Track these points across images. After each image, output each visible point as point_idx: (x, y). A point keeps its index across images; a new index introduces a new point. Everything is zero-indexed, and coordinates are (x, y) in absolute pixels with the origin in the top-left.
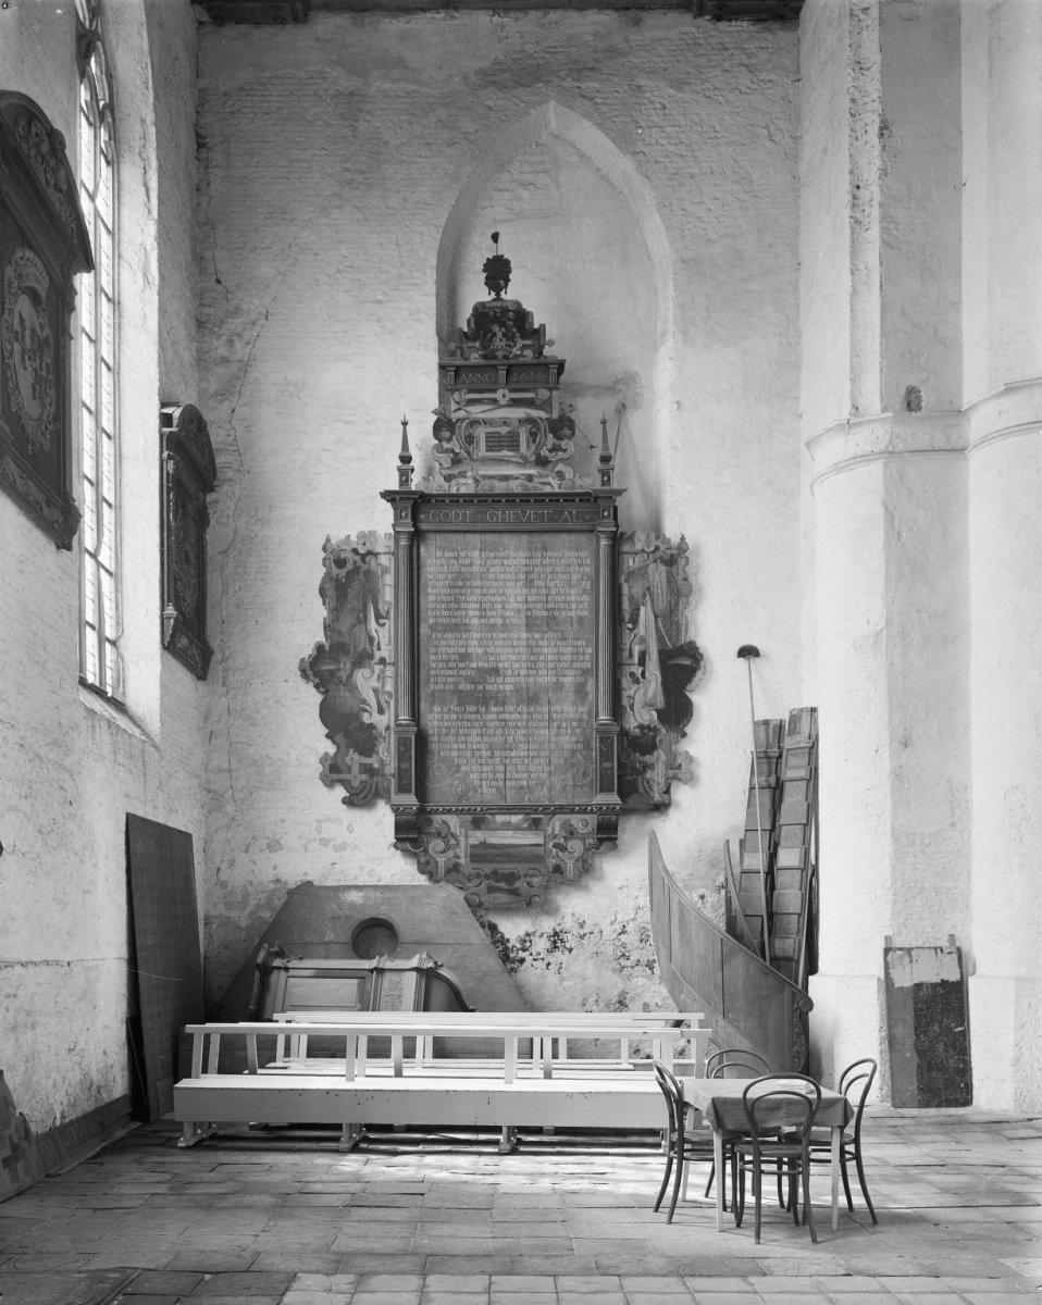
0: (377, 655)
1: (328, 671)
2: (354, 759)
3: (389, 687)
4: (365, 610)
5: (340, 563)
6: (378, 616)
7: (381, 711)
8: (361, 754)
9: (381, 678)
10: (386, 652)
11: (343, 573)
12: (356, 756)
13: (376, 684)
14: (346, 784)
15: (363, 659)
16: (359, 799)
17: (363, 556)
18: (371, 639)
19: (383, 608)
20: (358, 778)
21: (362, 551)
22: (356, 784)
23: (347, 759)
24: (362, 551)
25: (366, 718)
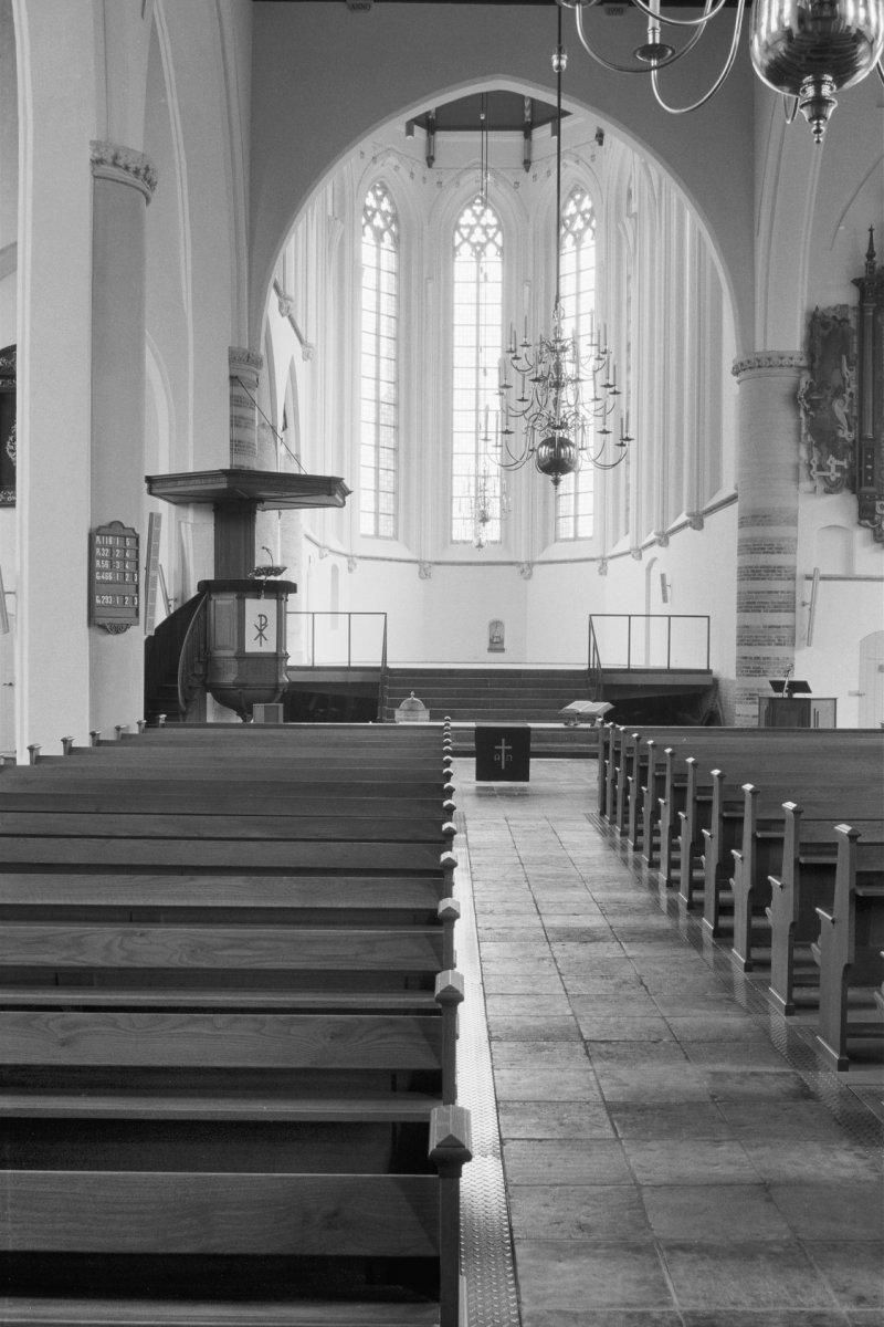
0: (848, 390)
1: (818, 400)
2: (832, 462)
3: (855, 413)
4: (840, 360)
5: (825, 325)
6: (849, 364)
7: (850, 430)
8: (837, 458)
9: (850, 406)
10: (853, 388)
11: (826, 333)
12: (831, 458)
13: (847, 411)
14: (825, 479)
15: (839, 392)
16: (831, 488)
17: (840, 322)
18: (844, 379)
19: (853, 358)
20: (834, 475)
21: (839, 318)
22: (833, 479)
23: (828, 462)
24: (839, 318)
25: (840, 434)
